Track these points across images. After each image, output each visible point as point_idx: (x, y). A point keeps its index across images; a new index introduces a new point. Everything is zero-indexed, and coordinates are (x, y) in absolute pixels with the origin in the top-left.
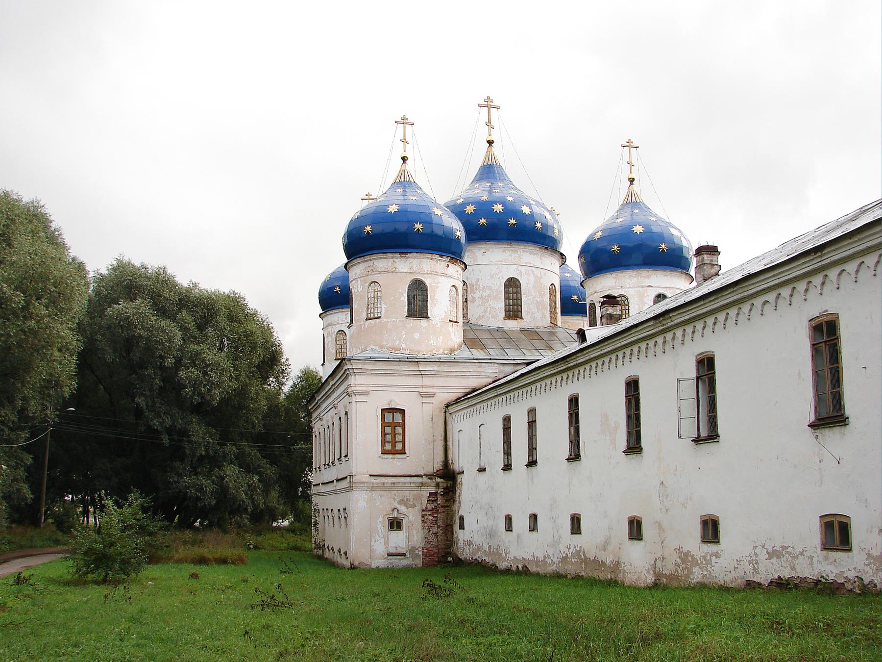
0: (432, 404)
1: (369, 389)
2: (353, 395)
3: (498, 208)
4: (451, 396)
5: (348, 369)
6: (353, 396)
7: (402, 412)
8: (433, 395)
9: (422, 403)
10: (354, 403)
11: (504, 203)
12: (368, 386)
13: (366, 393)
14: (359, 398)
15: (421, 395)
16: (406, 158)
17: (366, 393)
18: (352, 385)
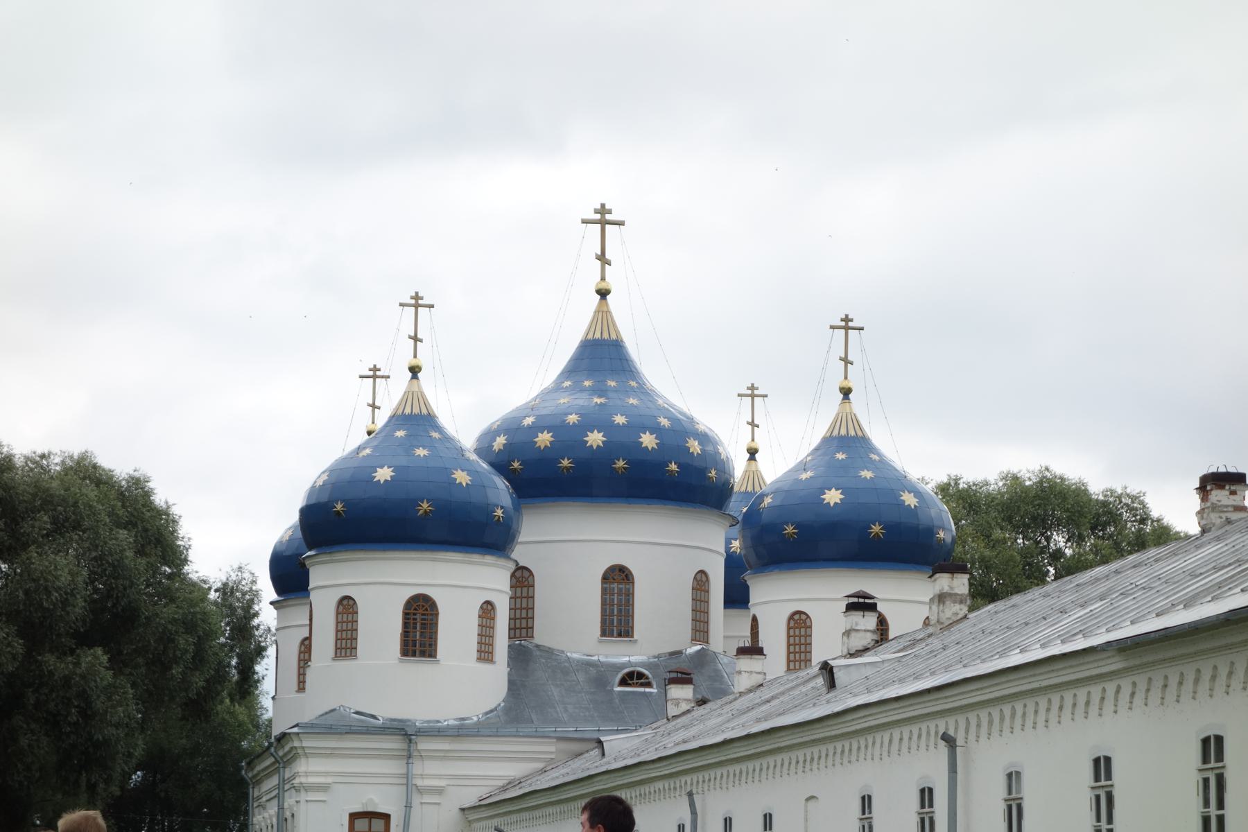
0: (437, 806)
1: (329, 780)
2: (302, 789)
3: (595, 439)
4: (470, 797)
5: (295, 747)
6: (303, 792)
7: (386, 817)
8: (439, 791)
9: (422, 803)
10: (303, 804)
11: (606, 426)
12: (327, 774)
13: (324, 788)
14: (312, 796)
15: (419, 790)
16: (417, 370)
17: (324, 788)
18: (300, 774)
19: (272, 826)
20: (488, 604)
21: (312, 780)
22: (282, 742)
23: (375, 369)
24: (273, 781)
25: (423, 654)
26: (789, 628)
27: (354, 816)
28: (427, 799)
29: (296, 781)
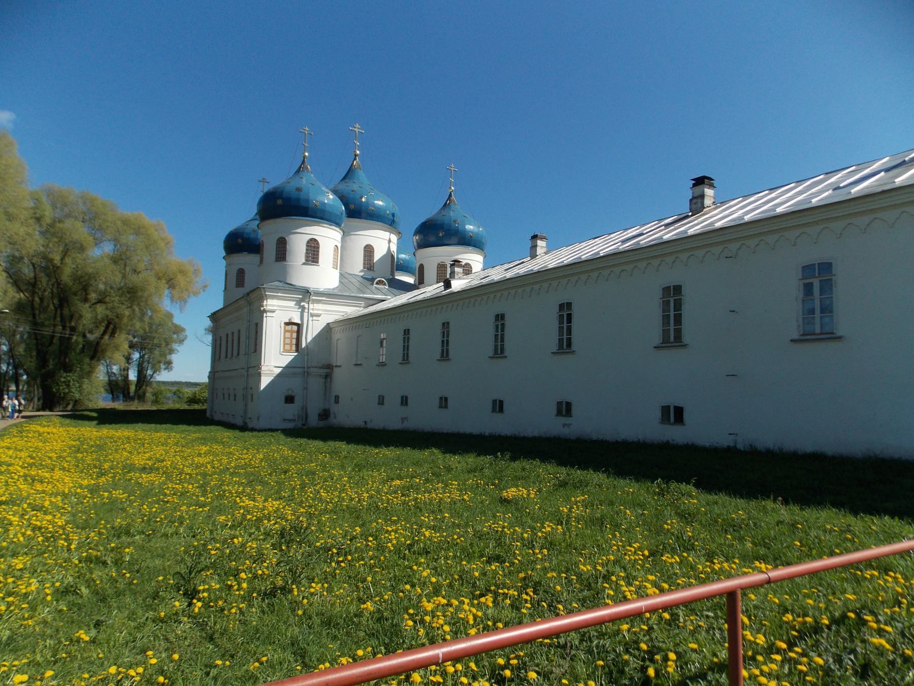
1: (275, 308)
8: (318, 315)
10: (265, 319)
13: (273, 311)
14: (269, 314)
17: (273, 311)
19: (233, 333)
20: (336, 246)
21: (269, 308)
22: (251, 295)
23: (264, 179)
24: (246, 310)
25: (313, 262)
26: (438, 268)
27: (287, 324)
28: (315, 318)
29: (262, 308)
